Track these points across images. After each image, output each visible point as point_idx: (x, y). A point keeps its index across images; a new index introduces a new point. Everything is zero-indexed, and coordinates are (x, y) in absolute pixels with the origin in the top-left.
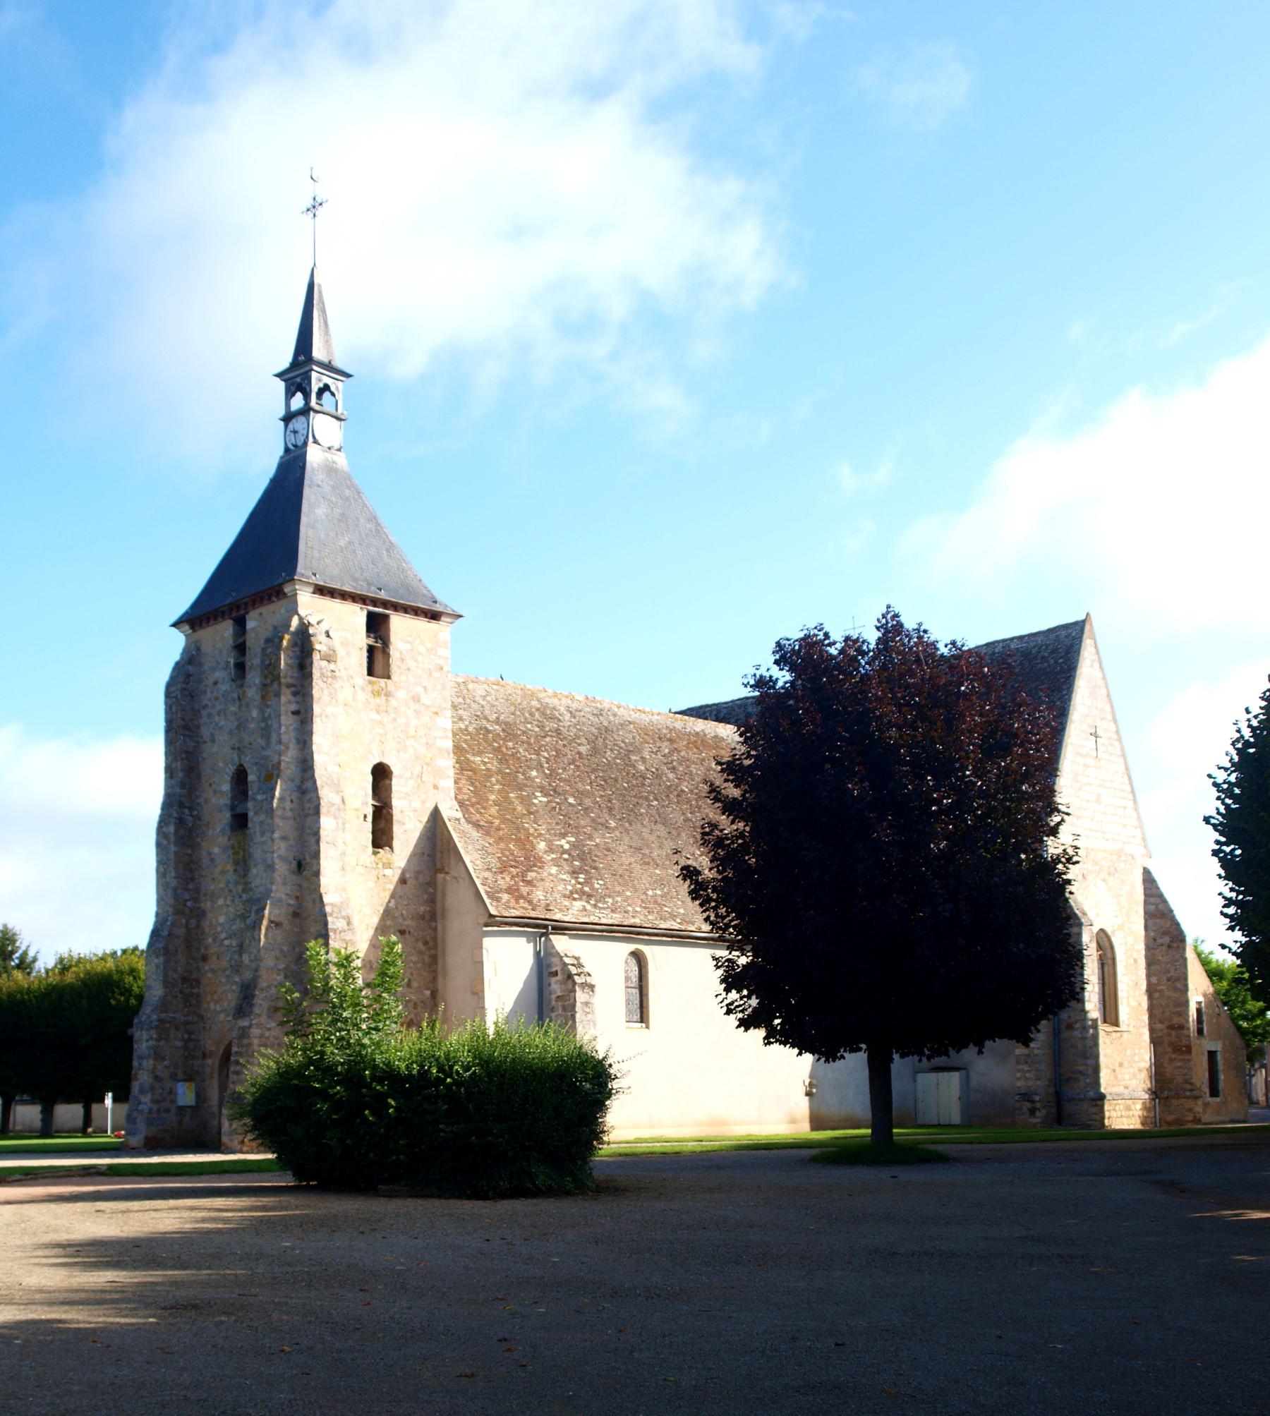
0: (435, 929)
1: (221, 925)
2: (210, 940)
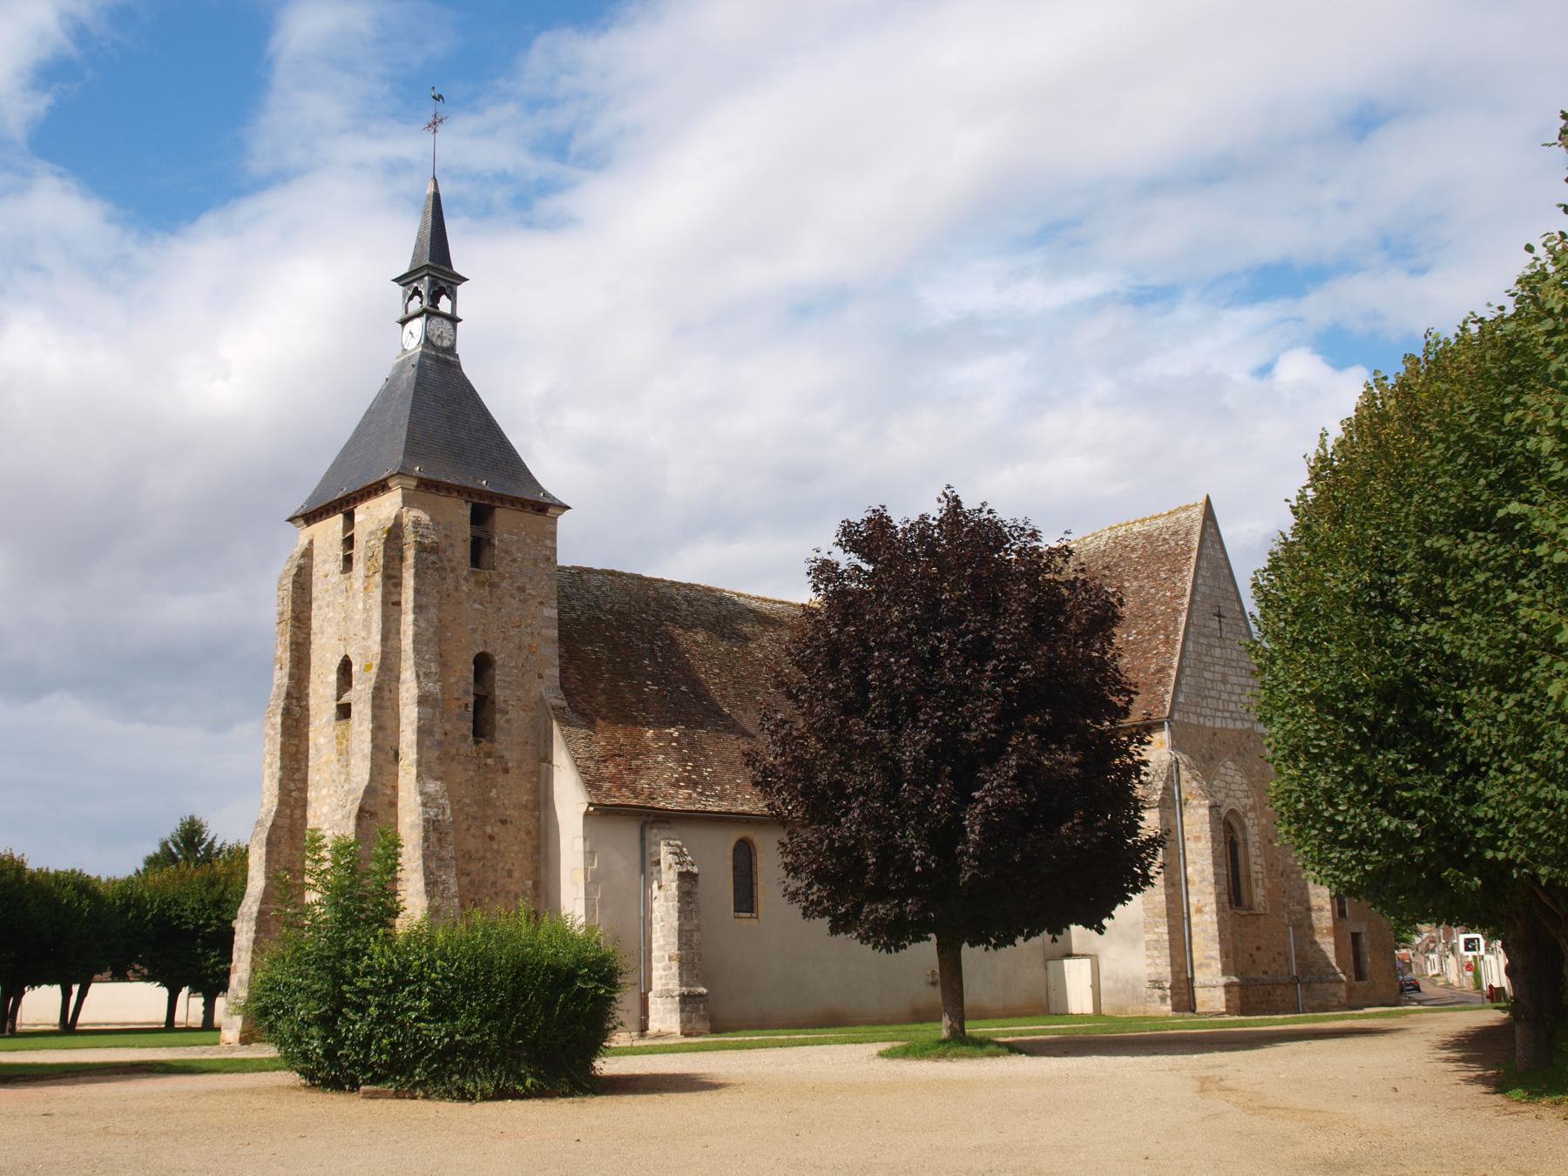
0: (538, 819)
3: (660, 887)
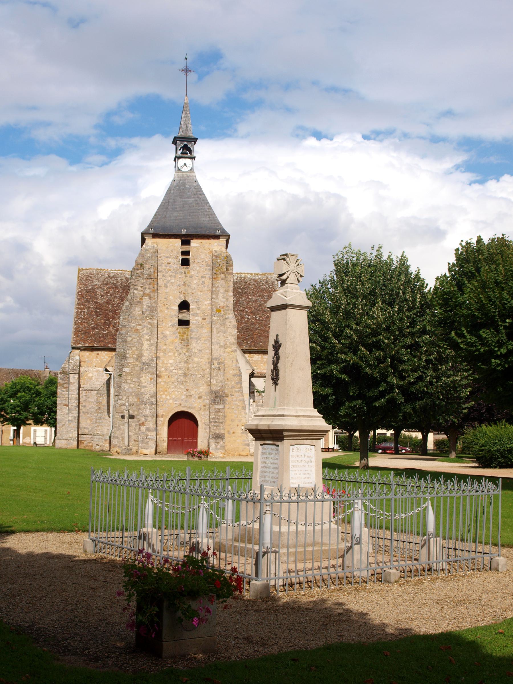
1: (171, 364)
2: (163, 369)
3: (254, 401)
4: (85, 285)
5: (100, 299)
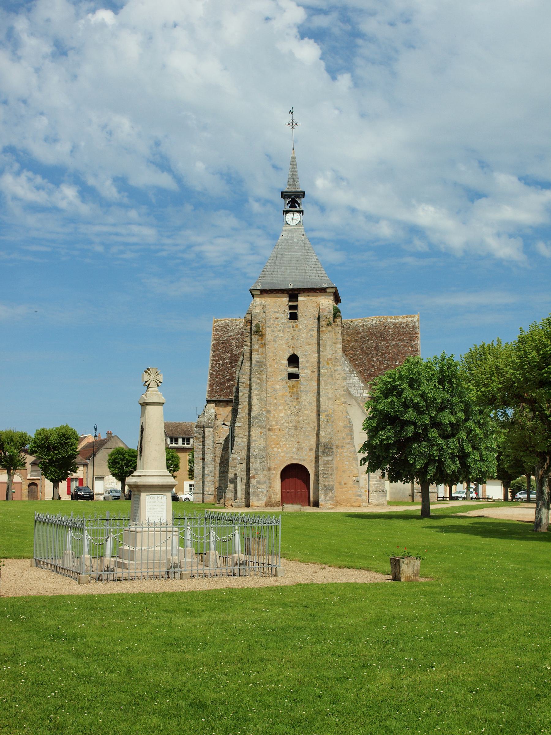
2: (274, 423)
4: (220, 336)
5: (235, 350)
